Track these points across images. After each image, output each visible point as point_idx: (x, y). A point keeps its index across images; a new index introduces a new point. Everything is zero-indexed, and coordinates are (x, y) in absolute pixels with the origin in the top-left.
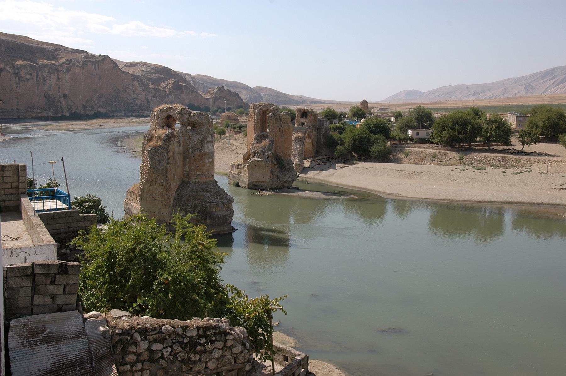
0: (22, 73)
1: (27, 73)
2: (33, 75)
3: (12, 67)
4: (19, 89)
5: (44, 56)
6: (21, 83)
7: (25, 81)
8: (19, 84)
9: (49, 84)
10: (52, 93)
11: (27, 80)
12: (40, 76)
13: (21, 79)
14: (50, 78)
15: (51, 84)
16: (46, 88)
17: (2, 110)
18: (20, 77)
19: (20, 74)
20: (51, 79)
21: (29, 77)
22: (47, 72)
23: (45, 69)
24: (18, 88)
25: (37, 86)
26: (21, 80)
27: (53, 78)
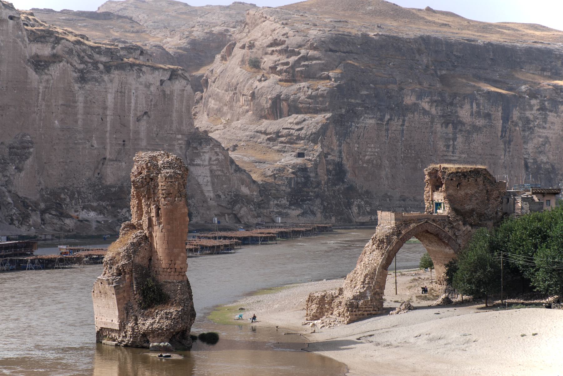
1: (478, 113)
2: (493, 117)
3: (435, 101)
4: (453, 152)
5: (543, 70)
6: (460, 139)
7: (469, 132)
8: (454, 139)
9: (540, 136)
10: (548, 158)
11: (476, 129)
12: (515, 119)
13: (459, 127)
14: (545, 121)
15: (547, 138)
16: (530, 147)
17: (404, 200)
18: (457, 124)
19: (458, 117)
20: (547, 126)
21: (480, 122)
22: (536, 108)
23: (534, 102)
24: (451, 149)
25: (505, 143)
26: (461, 130)
27: (552, 123)
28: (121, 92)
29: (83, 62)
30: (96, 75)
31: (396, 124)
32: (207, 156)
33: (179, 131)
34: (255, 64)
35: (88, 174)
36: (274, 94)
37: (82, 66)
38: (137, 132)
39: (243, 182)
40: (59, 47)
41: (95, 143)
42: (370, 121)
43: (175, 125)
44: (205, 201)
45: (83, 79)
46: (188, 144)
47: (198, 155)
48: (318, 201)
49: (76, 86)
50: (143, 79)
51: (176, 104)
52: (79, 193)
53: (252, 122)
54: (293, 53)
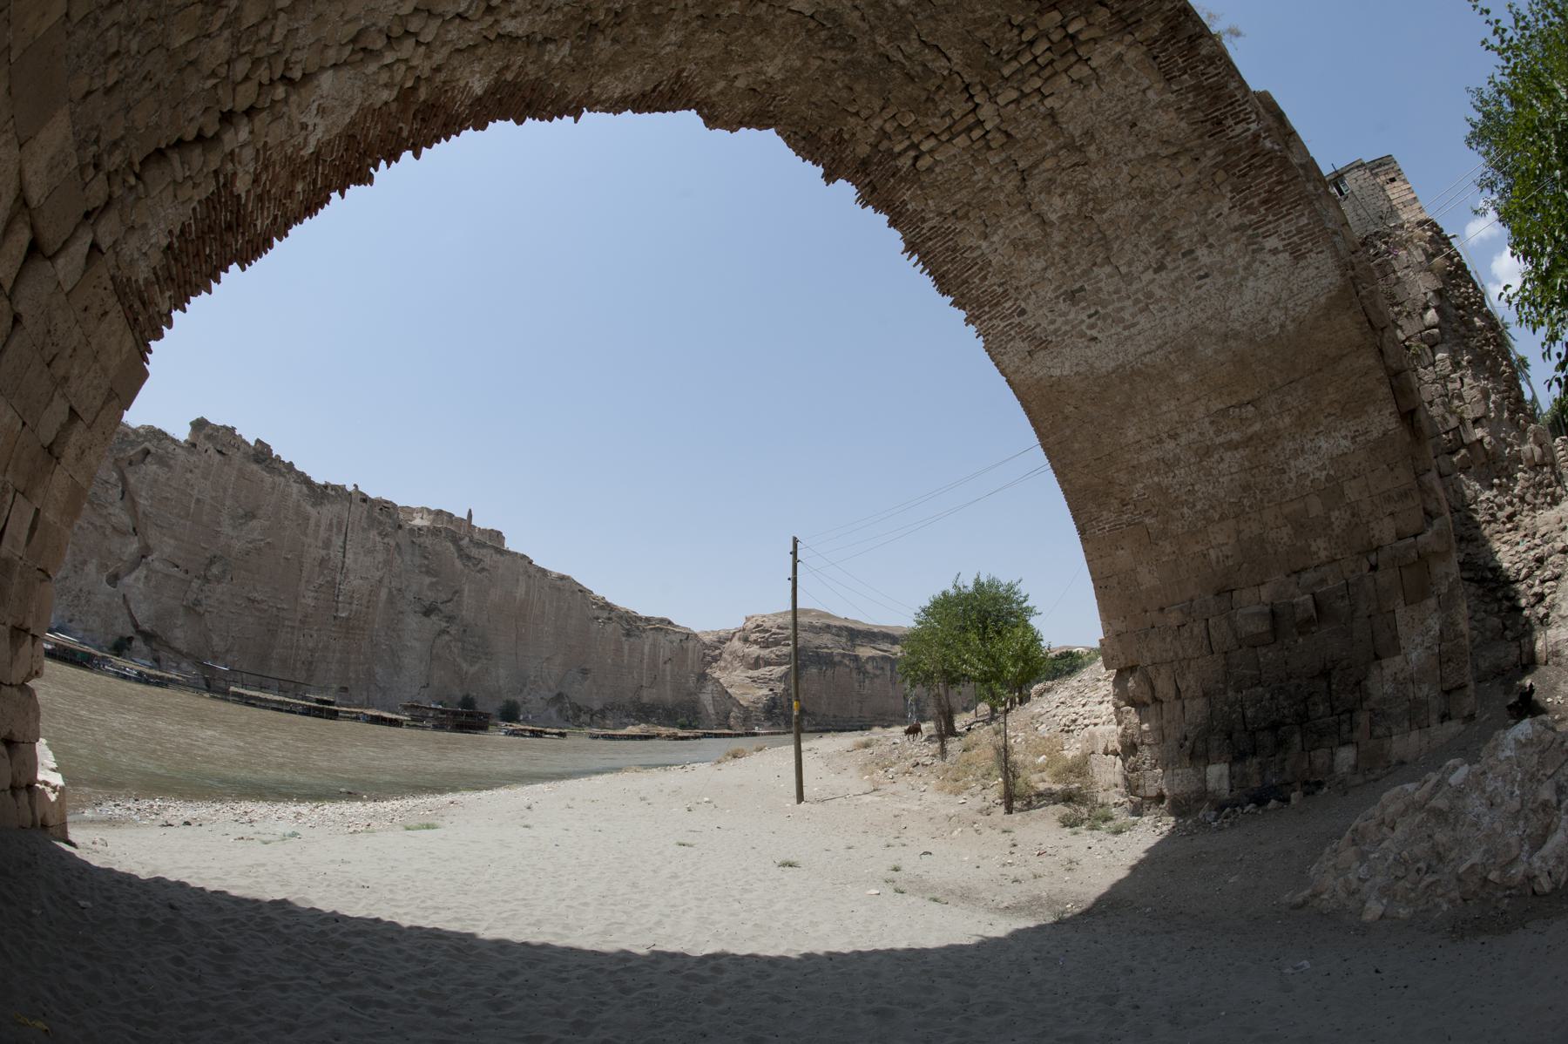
0: (869, 667)
6: (867, 681)
11: (876, 676)
18: (866, 673)
21: (878, 672)
28: (654, 645)
29: (628, 623)
30: (637, 633)
31: (829, 672)
32: (710, 688)
33: (693, 672)
34: (746, 640)
35: (630, 695)
36: (756, 655)
37: (628, 627)
38: (664, 671)
39: (734, 705)
40: (613, 614)
41: (636, 675)
42: (814, 670)
43: (690, 668)
44: (708, 716)
45: (628, 634)
46: (698, 680)
47: (704, 687)
48: (782, 717)
49: (624, 639)
50: (668, 638)
51: (690, 655)
52: (624, 706)
53: (742, 672)
54: (767, 631)
